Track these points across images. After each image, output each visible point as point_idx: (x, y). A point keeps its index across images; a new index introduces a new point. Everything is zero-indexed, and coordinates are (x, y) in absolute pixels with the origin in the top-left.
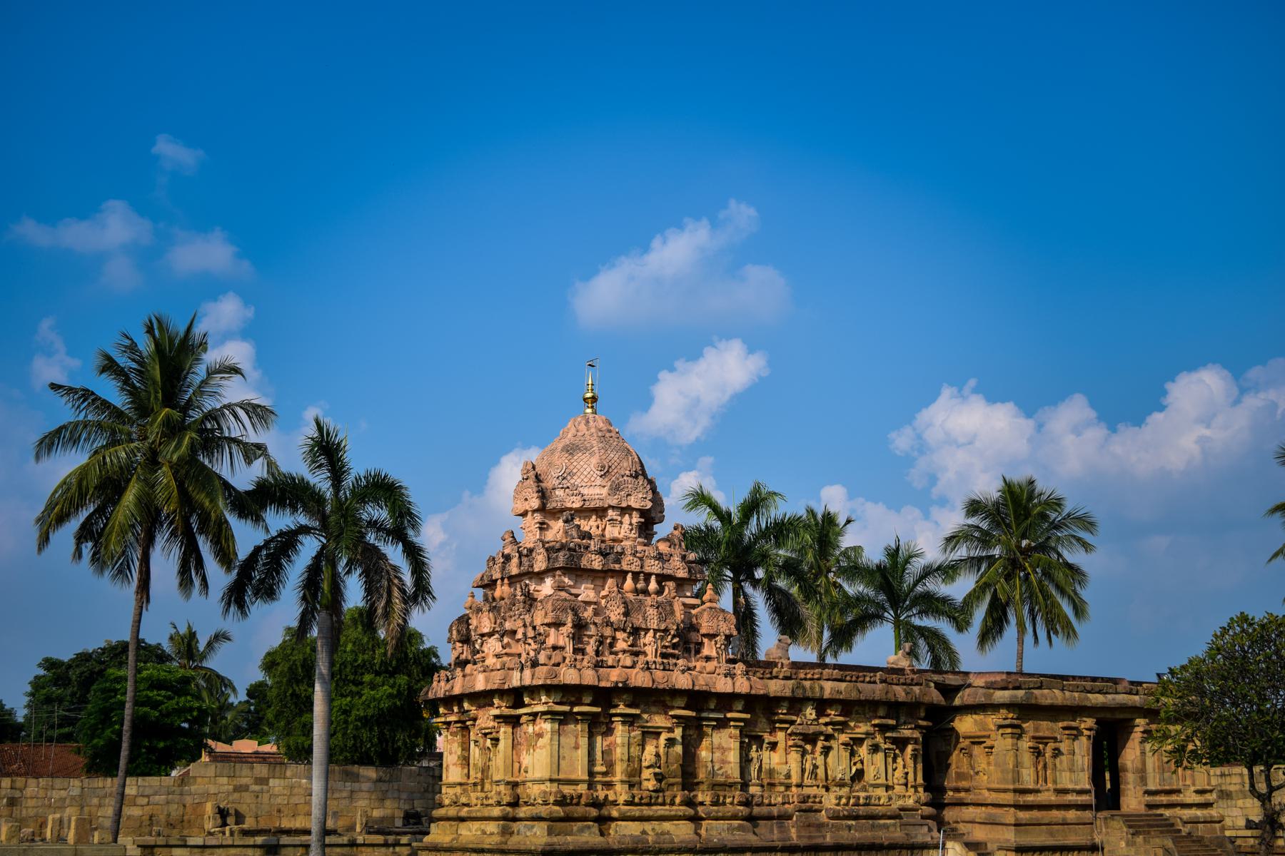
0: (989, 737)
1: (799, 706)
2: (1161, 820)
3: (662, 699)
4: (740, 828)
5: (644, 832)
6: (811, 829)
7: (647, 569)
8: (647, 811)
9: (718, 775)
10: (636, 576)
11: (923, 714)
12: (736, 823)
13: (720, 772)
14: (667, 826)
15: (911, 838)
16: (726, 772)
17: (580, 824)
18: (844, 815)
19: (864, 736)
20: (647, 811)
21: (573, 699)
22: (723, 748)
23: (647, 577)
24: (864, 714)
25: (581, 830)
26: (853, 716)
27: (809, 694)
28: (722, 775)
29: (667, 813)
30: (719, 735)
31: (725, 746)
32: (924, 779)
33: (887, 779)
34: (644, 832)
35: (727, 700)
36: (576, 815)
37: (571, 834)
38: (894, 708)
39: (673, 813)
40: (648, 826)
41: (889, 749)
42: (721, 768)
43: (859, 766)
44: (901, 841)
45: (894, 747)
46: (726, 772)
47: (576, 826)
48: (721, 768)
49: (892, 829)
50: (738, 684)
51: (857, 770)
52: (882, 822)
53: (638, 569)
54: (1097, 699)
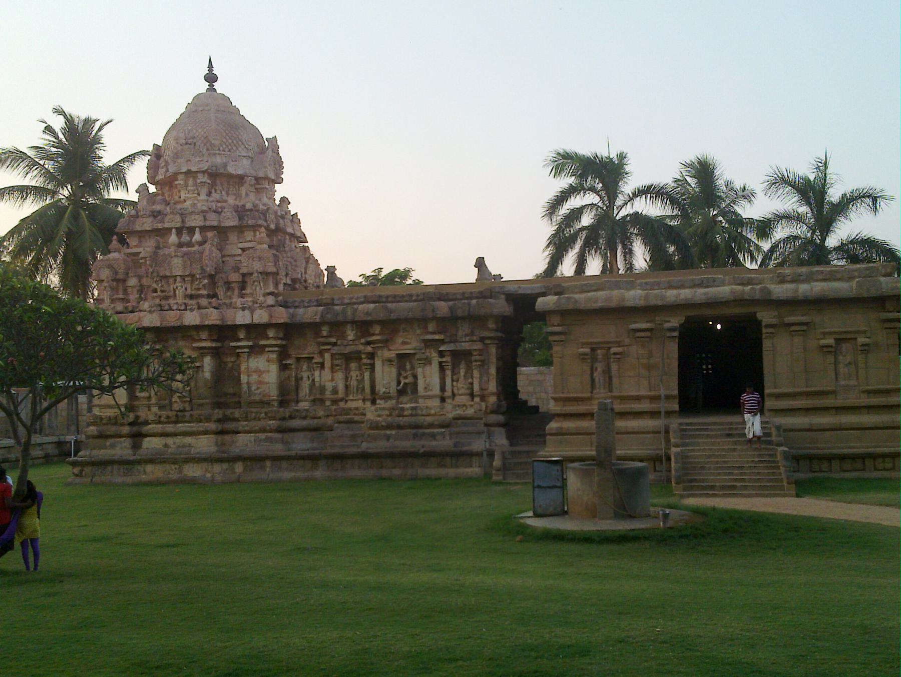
4: (267, 439)
5: (166, 446)
8: (170, 428)
9: (255, 394)
10: (179, 231)
12: (262, 436)
14: (189, 440)
16: (264, 391)
17: (112, 441)
18: (382, 426)
20: (170, 428)
22: (260, 371)
25: (113, 446)
26: (401, 333)
28: (260, 394)
29: (189, 429)
30: (256, 360)
34: (166, 446)
36: (108, 433)
40: (170, 441)
42: (258, 388)
48: (258, 388)
52: (427, 431)
53: (178, 225)
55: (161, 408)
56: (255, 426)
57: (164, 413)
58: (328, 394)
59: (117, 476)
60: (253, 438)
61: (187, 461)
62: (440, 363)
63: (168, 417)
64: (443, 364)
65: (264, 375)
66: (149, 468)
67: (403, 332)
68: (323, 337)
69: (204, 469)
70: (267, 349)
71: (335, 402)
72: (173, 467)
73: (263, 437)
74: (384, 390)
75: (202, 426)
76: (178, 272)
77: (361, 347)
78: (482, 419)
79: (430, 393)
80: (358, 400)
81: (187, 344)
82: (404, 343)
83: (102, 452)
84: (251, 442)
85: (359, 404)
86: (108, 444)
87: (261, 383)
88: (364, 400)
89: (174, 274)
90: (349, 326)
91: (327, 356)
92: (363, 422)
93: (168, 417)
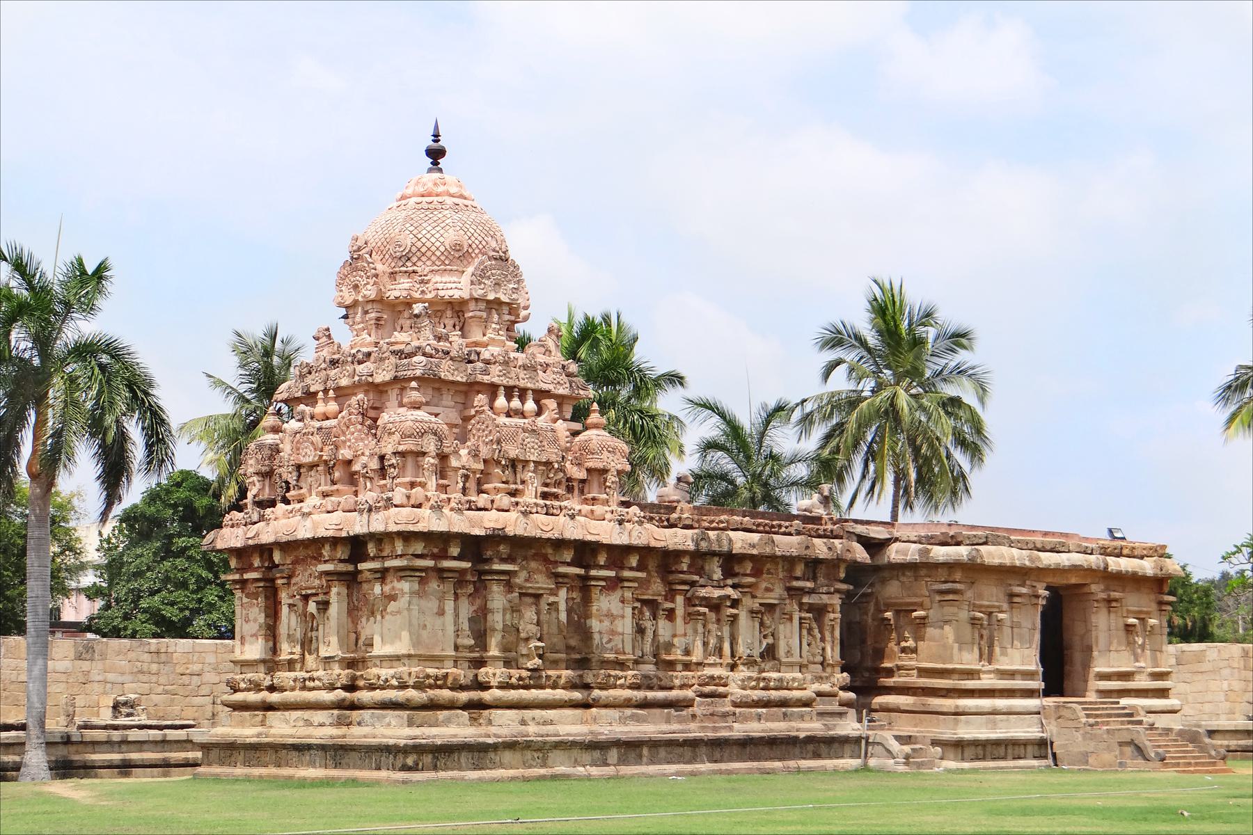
0: (921, 606)
1: (700, 562)
2: (1118, 708)
4: (632, 717)
11: (842, 575)
12: (629, 712)
13: (609, 646)
15: (830, 729)
16: (617, 645)
17: (446, 713)
18: (753, 701)
19: (776, 602)
21: (436, 550)
25: (447, 722)
27: (715, 548)
28: (612, 650)
30: (608, 598)
31: (615, 613)
32: (842, 657)
33: (801, 657)
35: (618, 554)
37: (436, 724)
38: (814, 565)
41: (805, 619)
42: (610, 641)
43: (770, 640)
44: (820, 733)
45: (810, 615)
46: (617, 645)
47: (442, 715)
48: (610, 641)
51: (768, 644)
54: (1048, 559)
57: (515, 673)
63: (520, 679)
65: (616, 622)
68: (682, 572)
69: (573, 760)
70: (626, 584)
74: (749, 651)
75: (560, 694)
77: (729, 591)
78: (835, 695)
81: (540, 567)
83: (434, 731)
84: (615, 720)
87: (613, 632)
90: (716, 559)
91: (680, 599)
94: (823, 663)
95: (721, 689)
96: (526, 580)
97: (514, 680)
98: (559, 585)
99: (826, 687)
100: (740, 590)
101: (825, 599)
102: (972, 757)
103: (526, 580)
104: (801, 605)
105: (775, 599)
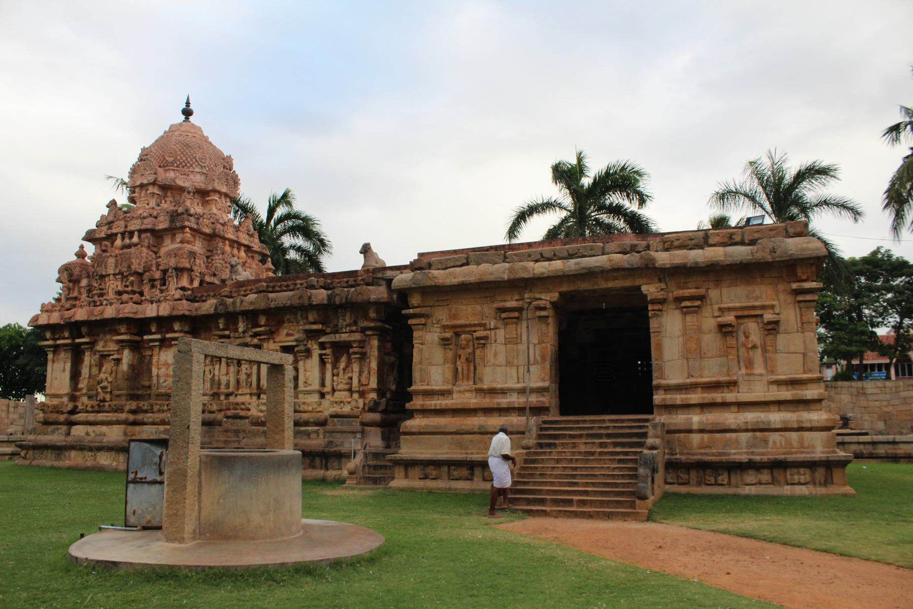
3: (114, 328)
5: (88, 434)
6: (229, 434)
7: (129, 229)
13: (165, 384)
14: (104, 429)
19: (294, 344)
22: (168, 364)
23: (131, 234)
24: (298, 323)
25: (53, 432)
26: (286, 325)
28: (166, 387)
29: (105, 419)
30: (166, 353)
34: (88, 434)
39: (114, 419)
42: (165, 381)
48: (165, 381)
49: (313, 436)
50: (161, 308)
53: (122, 230)
55: (90, 397)
56: (157, 418)
58: (223, 389)
59: (48, 460)
60: (154, 430)
61: (100, 449)
62: (321, 355)
64: (323, 357)
66: (73, 453)
67: (288, 323)
70: (173, 343)
71: (228, 395)
72: (90, 454)
73: (163, 429)
76: (112, 272)
79: (309, 388)
80: (246, 394)
82: (288, 335)
85: (246, 399)
86: (49, 429)
88: (251, 394)
89: (108, 273)
92: (247, 418)
93: (92, 407)
94: (350, 390)
95: (242, 413)
96: (103, 347)
97: (89, 408)
98: (123, 348)
99: (347, 409)
100: (258, 337)
101: (344, 337)
102: (422, 477)
103: (103, 347)
104: (322, 346)
105: (293, 341)
